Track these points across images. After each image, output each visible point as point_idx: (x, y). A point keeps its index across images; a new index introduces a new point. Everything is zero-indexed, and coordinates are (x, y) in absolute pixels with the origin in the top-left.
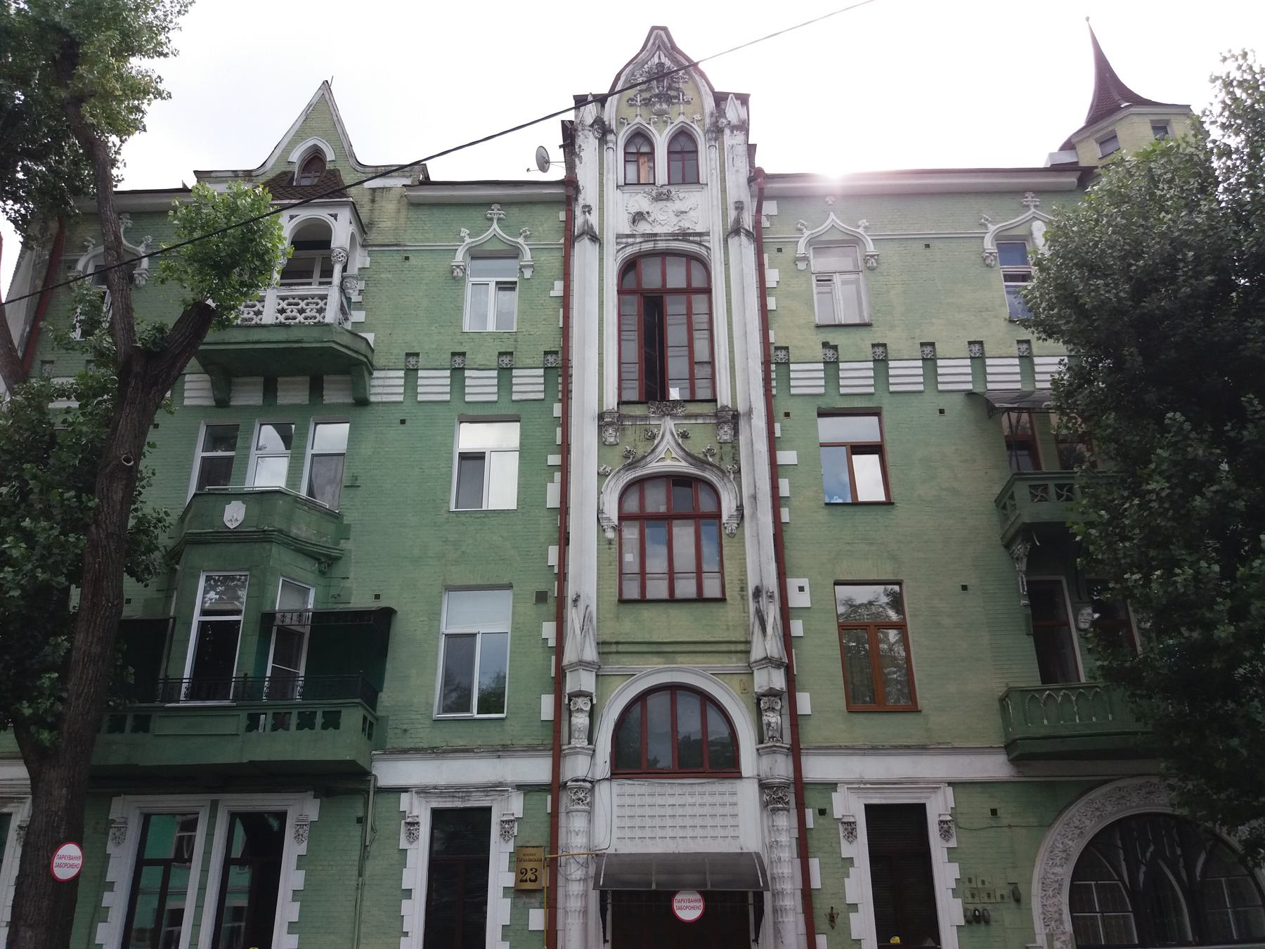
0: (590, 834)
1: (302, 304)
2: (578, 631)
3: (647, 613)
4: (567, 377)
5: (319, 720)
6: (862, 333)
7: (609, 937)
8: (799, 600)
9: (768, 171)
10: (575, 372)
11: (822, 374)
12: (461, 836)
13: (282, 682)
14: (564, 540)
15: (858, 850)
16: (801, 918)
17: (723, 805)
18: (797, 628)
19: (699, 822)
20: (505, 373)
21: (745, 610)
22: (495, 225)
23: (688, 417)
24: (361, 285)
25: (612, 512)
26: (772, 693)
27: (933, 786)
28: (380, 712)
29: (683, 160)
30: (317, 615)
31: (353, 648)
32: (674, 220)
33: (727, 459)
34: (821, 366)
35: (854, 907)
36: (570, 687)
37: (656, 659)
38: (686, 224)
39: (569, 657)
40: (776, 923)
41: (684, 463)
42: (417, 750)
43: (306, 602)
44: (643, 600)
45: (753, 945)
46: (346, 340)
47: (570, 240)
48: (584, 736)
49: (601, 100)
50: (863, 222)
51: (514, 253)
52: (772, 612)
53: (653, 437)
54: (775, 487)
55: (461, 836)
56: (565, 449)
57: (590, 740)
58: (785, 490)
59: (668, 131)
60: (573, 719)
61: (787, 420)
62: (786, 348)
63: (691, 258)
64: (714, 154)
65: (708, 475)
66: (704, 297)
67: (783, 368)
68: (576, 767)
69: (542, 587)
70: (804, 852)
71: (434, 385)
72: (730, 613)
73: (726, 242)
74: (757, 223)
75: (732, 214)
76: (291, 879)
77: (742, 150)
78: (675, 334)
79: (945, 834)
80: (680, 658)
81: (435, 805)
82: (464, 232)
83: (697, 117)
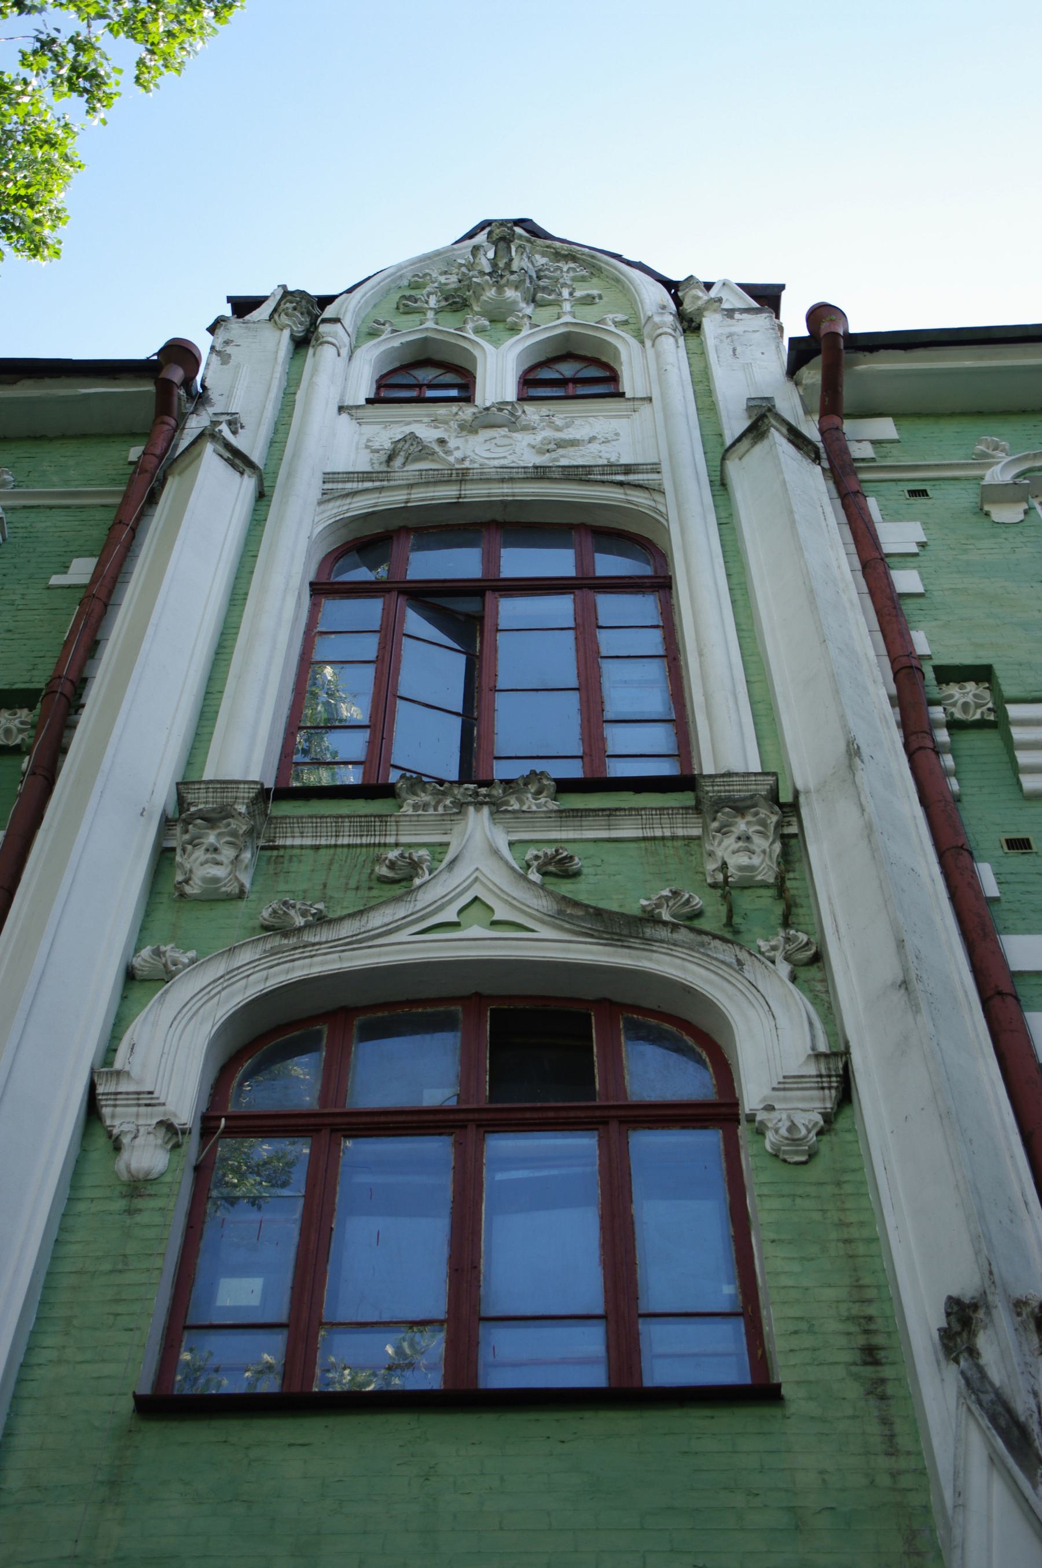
61: (1017, 860)
62: (982, 674)
65: (668, 963)
66: (643, 607)
73: (721, 485)
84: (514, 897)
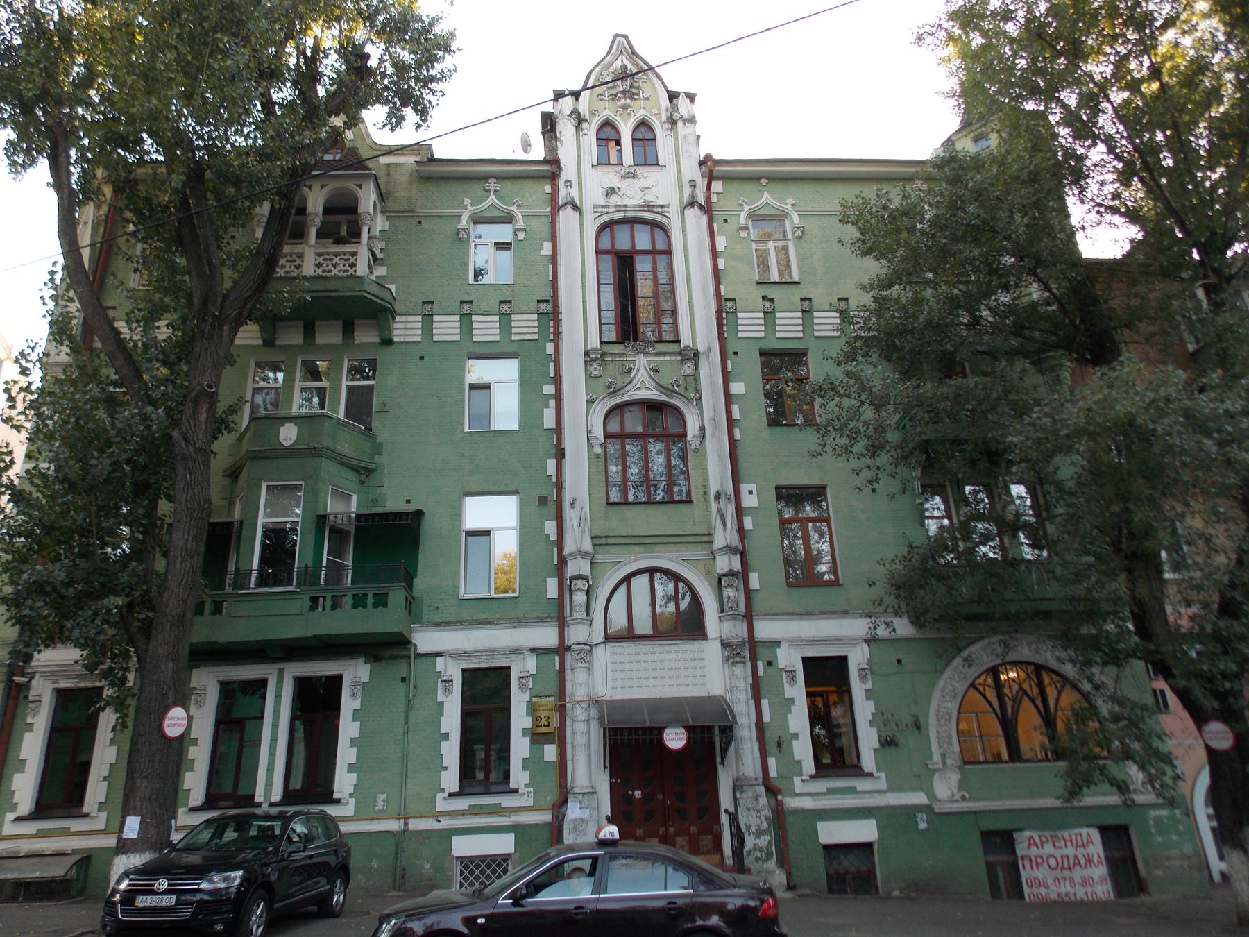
0: (589, 685)
1: (336, 260)
2: (576, 528)
3: (630, 512)
4: (557, 321)
5: (370, 601)
6: (793, 288)
7: (607, 764)
8: (749, 501)
9: (716, 157)
10: (563, 316)
11: (762, 322)
12: (486, 691)
13: (335, 570)
14: (560, 455)
15: (797, 691)
16: (756, 746)
17: (678, 660)
18: (748, 523)
19: (673, 673)
20: (505, 317)
21: (708, 509)
22: (492, 196)
23: (658, 354)
24: (383, 245)
25: (599, 432)
26: (731, 573)
27: (853, 641)
28: (416, 593)
29: (644, 146)
30: (359, 516)
31: (391, 543)
32: (641, 194)
33: (691, 389)
34: (762, 315)
35: (796, 736)
36: (571, 569)
37: (637, 549)
38: (650, 198)
39: (569, 548)
40: (737, 750)
41: (655, 392)
42: (448, 623)
43: (349, 506)
44: (626, 503)
45: (720, 768)
46: (375, 289)
47: (556, 209)
48: (583, 609)
49: (576, 95)
50: (791, 201)
51: (508, 219)
52: (730, 511)
53: (630, 371)
54: (729, 412)
55: (486, 691)
56: (557, 381)
57: (588, 614)
58: (736, 415)
59: (632, 122)
60: (574, 597)
61: (735, 359)
62: (734, 300)
63: (654, 225)
64: (670, 141)
65: (675, 402)
67: (731, 317)
68: (576, 634)
69: (544, 493)
70: (757, 694)
71: (447, 327)
72: (696, 511)
73: (683, 212)
74: (708, 198)
75: (687, 191)
76: (348, 728)
77: (692, 139)
78: (644, 288)
79: (863, 678)
80: (657, 548)
81: (465, 666)
82: (467, 201)
83: (655, 111)
84: (649, 383)
